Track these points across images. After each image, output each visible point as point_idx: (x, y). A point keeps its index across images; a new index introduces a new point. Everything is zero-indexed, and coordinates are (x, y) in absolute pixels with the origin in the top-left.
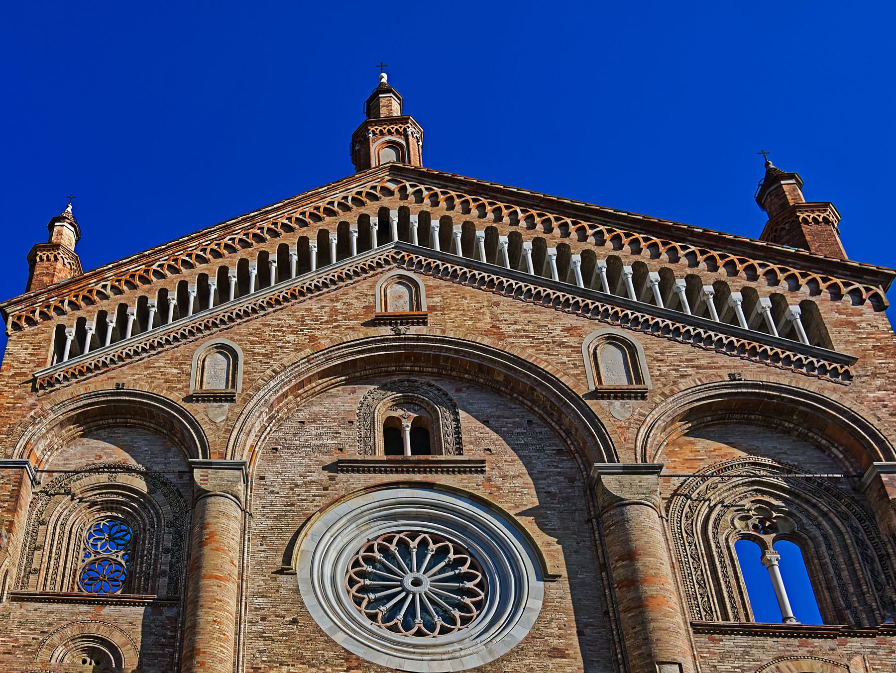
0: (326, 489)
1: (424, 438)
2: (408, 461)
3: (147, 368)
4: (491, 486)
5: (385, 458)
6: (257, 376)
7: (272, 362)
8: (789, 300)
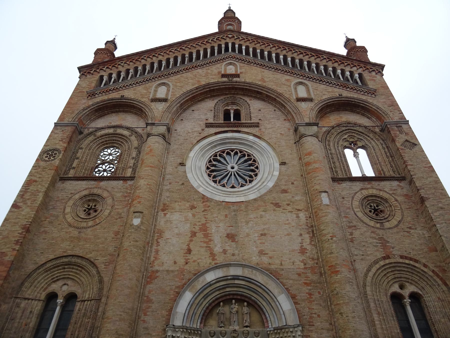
0: (200, 134)
1: (237, 115)
2: (231, 123)
3: (134, 90)
4: (261, 132)
5: (223, 122)
6: (176, 93)
7: (183, 89)
8: (355, 73)
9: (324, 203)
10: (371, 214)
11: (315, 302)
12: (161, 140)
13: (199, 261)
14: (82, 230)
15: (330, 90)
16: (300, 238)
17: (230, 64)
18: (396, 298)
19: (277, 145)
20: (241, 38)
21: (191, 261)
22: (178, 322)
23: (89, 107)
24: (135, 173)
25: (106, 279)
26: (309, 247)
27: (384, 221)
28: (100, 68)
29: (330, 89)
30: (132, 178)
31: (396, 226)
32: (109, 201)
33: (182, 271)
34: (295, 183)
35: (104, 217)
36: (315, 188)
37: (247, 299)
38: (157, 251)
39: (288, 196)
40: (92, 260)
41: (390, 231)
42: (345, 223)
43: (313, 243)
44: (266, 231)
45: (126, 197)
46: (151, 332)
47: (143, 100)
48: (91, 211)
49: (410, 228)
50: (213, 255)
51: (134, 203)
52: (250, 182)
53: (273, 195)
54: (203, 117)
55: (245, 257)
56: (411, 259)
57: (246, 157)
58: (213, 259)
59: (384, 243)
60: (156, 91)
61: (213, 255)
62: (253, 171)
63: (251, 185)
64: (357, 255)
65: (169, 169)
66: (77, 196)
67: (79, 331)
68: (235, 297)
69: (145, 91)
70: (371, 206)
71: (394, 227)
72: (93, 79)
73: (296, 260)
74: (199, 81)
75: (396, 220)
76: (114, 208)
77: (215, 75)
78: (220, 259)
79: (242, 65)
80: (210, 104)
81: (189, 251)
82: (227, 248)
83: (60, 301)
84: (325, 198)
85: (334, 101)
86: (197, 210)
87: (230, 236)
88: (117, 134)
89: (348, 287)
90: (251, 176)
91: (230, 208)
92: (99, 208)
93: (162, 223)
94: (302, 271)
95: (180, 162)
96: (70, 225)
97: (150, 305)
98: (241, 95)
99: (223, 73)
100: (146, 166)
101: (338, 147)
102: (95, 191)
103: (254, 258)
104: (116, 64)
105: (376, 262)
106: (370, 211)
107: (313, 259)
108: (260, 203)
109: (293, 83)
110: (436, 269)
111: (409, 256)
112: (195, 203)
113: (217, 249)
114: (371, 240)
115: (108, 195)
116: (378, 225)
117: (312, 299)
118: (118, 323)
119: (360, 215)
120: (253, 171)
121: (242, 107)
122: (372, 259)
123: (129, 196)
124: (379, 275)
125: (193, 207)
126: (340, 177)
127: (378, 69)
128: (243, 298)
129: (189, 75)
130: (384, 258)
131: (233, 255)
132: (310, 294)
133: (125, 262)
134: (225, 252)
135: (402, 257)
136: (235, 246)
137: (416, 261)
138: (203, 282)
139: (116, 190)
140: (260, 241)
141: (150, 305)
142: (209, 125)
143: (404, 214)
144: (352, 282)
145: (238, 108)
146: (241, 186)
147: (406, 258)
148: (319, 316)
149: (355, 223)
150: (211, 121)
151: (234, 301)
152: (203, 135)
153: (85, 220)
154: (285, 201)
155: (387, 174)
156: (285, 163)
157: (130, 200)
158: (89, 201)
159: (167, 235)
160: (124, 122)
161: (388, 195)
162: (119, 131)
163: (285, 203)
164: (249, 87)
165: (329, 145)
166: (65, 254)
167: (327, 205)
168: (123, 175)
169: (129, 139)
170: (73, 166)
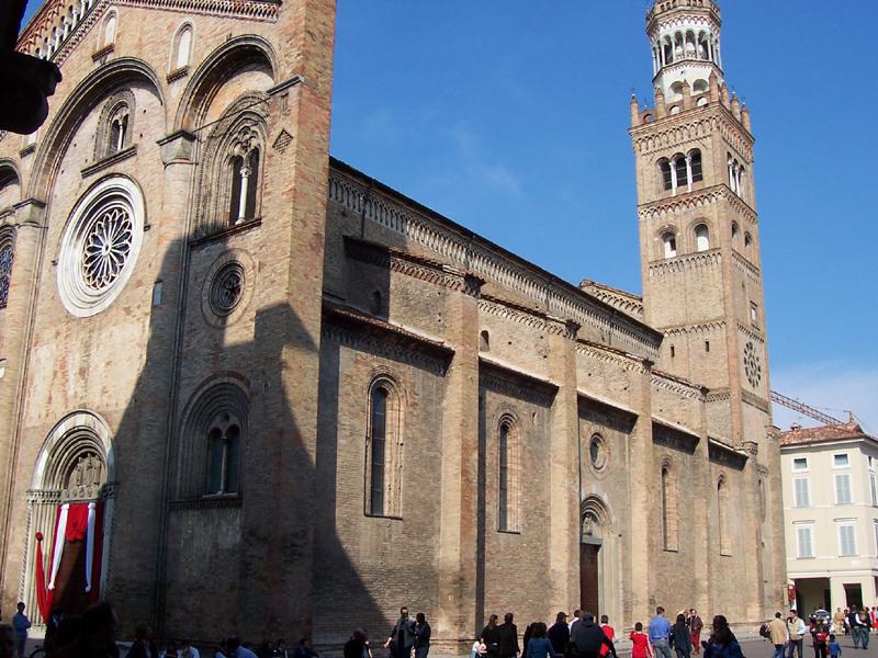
58: (66, 408)
80: (92, 123)
81: (50, 398)
131: (81, 398)
142: (86, 173)
152: (78, 197)
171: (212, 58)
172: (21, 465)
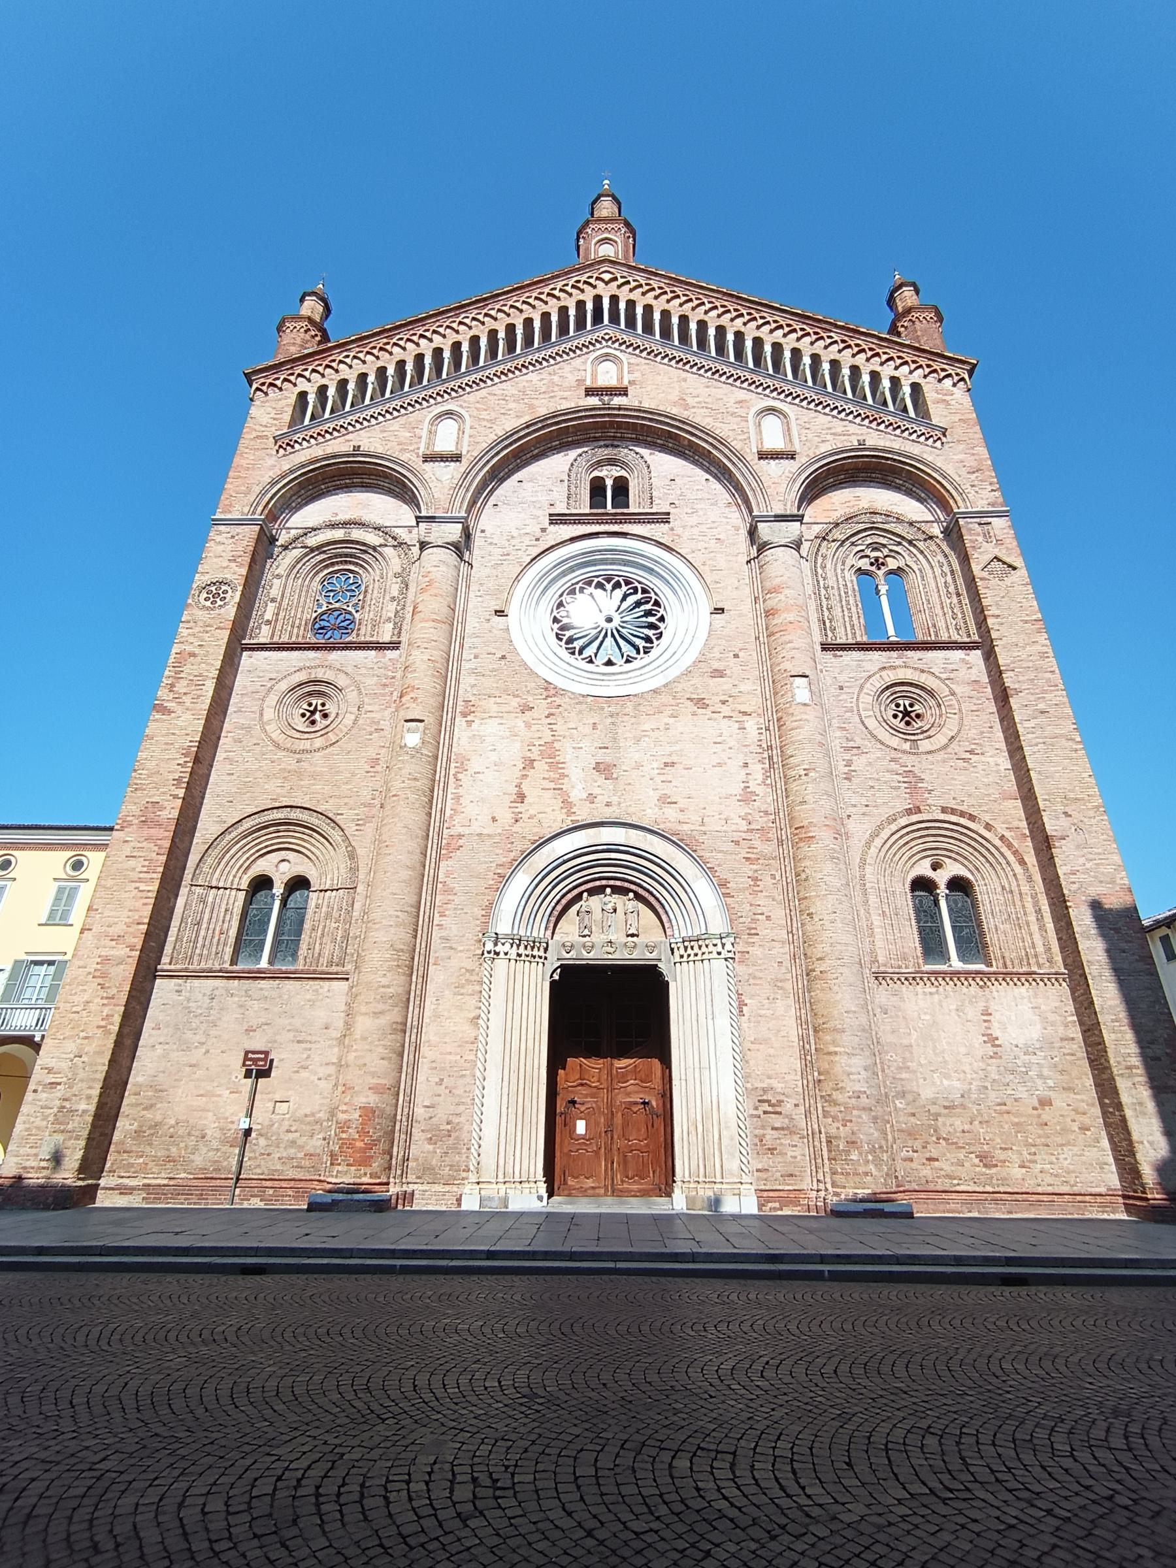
0: (537, 540)
3: (382, 431)
5: (588, 511)
6: (481, 439)
9: (798, 701)
10: (896, 722)
11: (764, 894)
12: (450, 556)
13: (541, 816)
14: (304, 756)
15: (839, 430)
16: (744, 771)
17: (606, 357)
18: (922, 885)
19: (707, 568)
20: (633, 284)
21: (525, 816)
22: (504, 928)
23: (283, 477)
24: (400, 633)
25: (360, 851)
26: (760, 790)
27: (921, 737)
28: (297, 372)
29: (839, 426)
30: (394, 645)
31: (945, 747)
32: (352, 696)
33: (509, 837)
34: (741, 654)
35: (345, 730)
36: (782, 667)
37: (633, 887)
38: (457, 798)
39: (724, 684)
40: (330, 815)
41: (929, 756)
42: (838, 741)
43: (768, 782)
44: (674, 758)
45: (385, 685)
46: (454, 946)
47: (405, 457)
48: (317, 716)
49: (971, 752)
50: (567, 804)
51: (404, 699)
52: (645, 653)
53: (692, 682)
54: (544, 499)
55: (630, 810)
56: (962, 814)
57: (639, 596)
58: (569, 813)
59: (913, 782)
60: (432, 433)
61: (567, 804)
62: (652, 626)
63: (647, 659)
64: (855, 806)
65: (472, 624)
66: (284, 686)
67: (321, 944)
68: (612, 882)
69: (408, 434)
70: (898, 705)
71: (939, 750)
72: (284, 402)
73: (732, 815)
74: (531, 407)
75: (945, 735)
76: (363, 710)
77: (570, 389)
78: (583, 816)
79: (634, 360)
80: (558, 463)
81: (521, 797)
82: (596, 791)
83: (278, 890)
84: (801, 691)
85: (844, 458)
86: (535, 714)
87: (602, 766)
88: (352, 542)
89: (828, 867)
90: (648, 639)
91: (603, 709)
92: (330, 708)
93: (464, 741)
94: (744, 835)
95: (498, 608)
96: (277, 746)
97: (450, 897)
98: (631, 440)
99: (588, 383)
100: (423, 620)
101: (843, 570)
102: (320, 674)
103: (649, 811)
104: (334, 361)
105: (892, 819)
106: (895, 716)
107: (766, 813)
108: (665, 698)
109: (753, 410)
110: (1008, 834)
111: (960, 808)
112: (530, 699)
113: (577, 794)
114: (888, 775)
115: (348, 682)
116: (907, 746)
117: (756, 889)
118: (393, 930)
119: (872, 723)
120: (652, 626)
121: (632, 470)
122: (885, 812)
123: (392, 685)
124: (894, 843)
125: (526, 708)
126: (839, 641)
127: (959, 371)
128: (626, 885)
129: (507, 388)
130: (909, 812)
131: (608, 804)
132: (756, 879)
133: (396, 820)
134: (591, 798)
135: (944, 810)
136: (611, 787)
137: (972, 818)
138: (549, 856)
139: (363, 671)
140: (662, 778)
141: (450, 897)
142: (557, 519)
143: (965, 723)
144: (838, 858)
145: (623, 473)
146: (627, 661)
147: (953, 811)
148: (768, 918)
149: (858, 742)
150: (561, 508)
151: (608, 890)
153: (306, 736)
154: (717, 694)
155: (944, 637)
156: (723, 610)
157: (395, 694)
158: (310, 694)
159: (475, 765)
160: (366, 511)
161: (938, 681)
162: (357, 534)
163: (717, 699)
164: (651, 420)
165: (824, 567)
166: (277, 805)
167: (805, 705)
168: (374, 639)
169: (380, 554)
170: (266, 618)
171: (831, 455)
172: (449, 891)
